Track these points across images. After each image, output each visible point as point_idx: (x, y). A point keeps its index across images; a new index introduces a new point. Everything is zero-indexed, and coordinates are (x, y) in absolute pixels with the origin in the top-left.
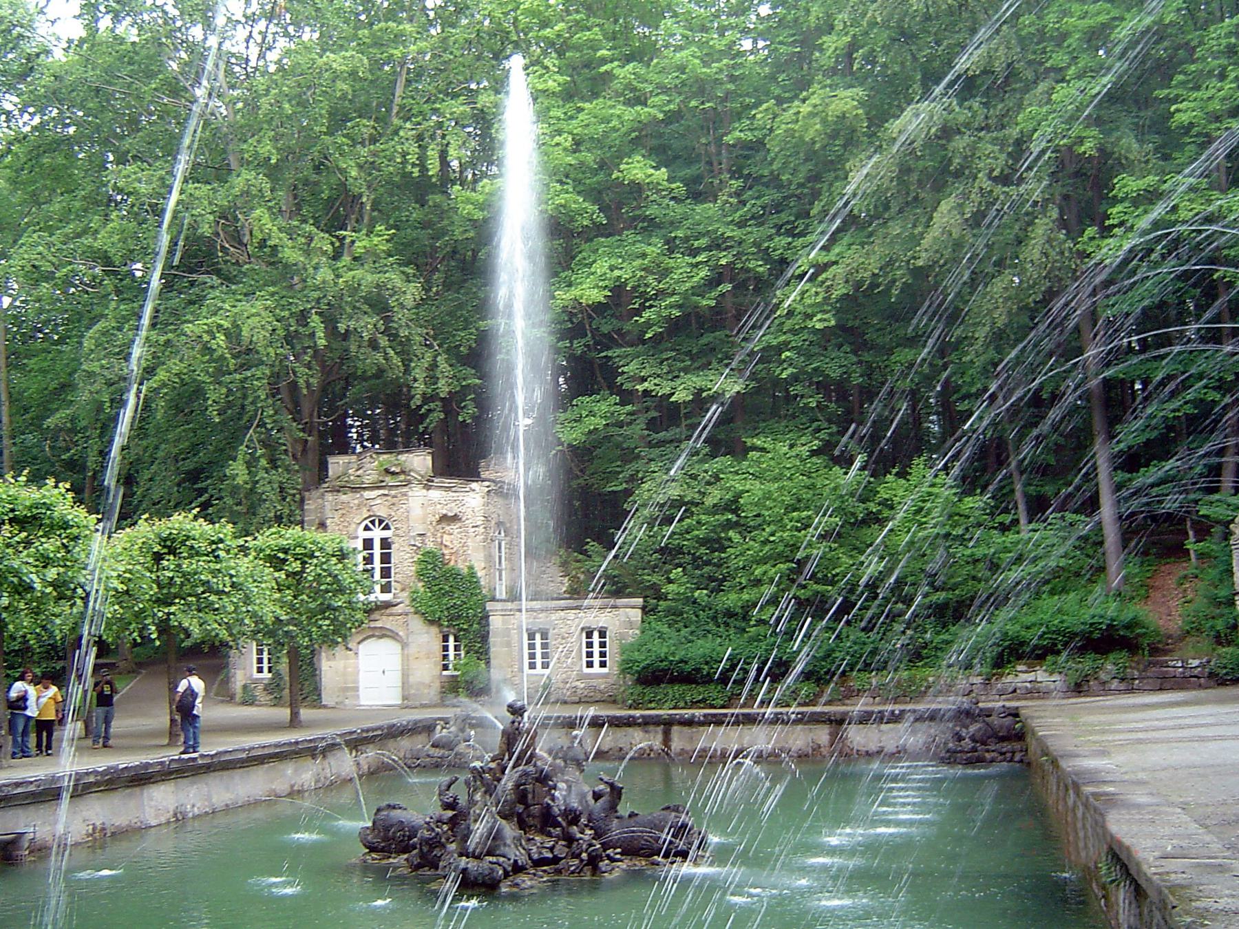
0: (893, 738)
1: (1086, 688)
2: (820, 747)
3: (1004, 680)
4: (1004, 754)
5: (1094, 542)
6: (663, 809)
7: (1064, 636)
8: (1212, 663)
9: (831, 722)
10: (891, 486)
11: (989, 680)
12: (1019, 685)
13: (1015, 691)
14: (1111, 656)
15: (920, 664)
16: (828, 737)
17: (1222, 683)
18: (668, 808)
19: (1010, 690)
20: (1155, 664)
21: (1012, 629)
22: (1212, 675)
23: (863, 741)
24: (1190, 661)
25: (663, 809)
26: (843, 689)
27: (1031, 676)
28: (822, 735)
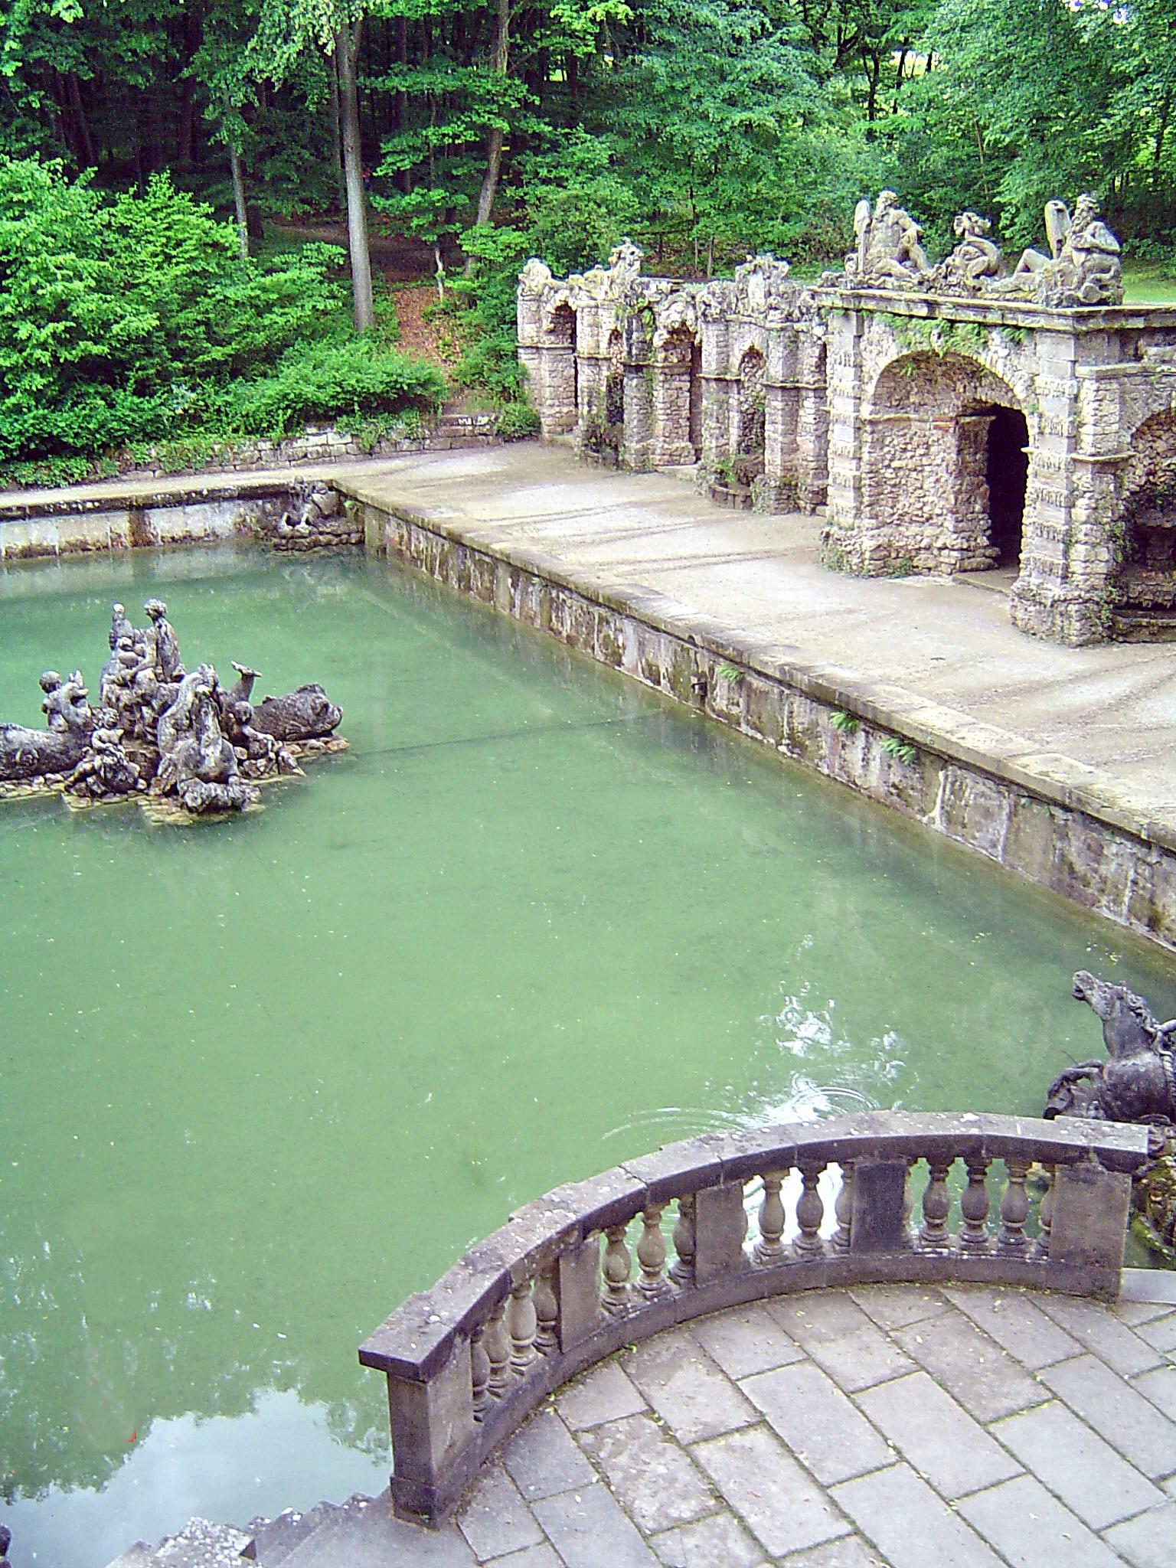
0: (199, 521)
1: (377, 449)
2: (119, 536)
3: (295, 444)
4: (340, 535)
5: (340, 272)
6: (299, 692)
7: (359, 396)
8: (500, 420)
9: (131, 507)
10: (126, 208)
11: (279, 445)
12: (310, 449)
13: (306, 456)
14: (403, 415)
15: (202, 429)
16: (128, 524)
17: (509, 440)
18: (304, 689)
19: (300, 455)
20: (445, 422)
21: (309, 391)
22: (499, 433)
23: (167, 526)
24: (480, 418)
25: (299, 692)
26: (118, 463)
27: (322, 439)
28: (122, 523)
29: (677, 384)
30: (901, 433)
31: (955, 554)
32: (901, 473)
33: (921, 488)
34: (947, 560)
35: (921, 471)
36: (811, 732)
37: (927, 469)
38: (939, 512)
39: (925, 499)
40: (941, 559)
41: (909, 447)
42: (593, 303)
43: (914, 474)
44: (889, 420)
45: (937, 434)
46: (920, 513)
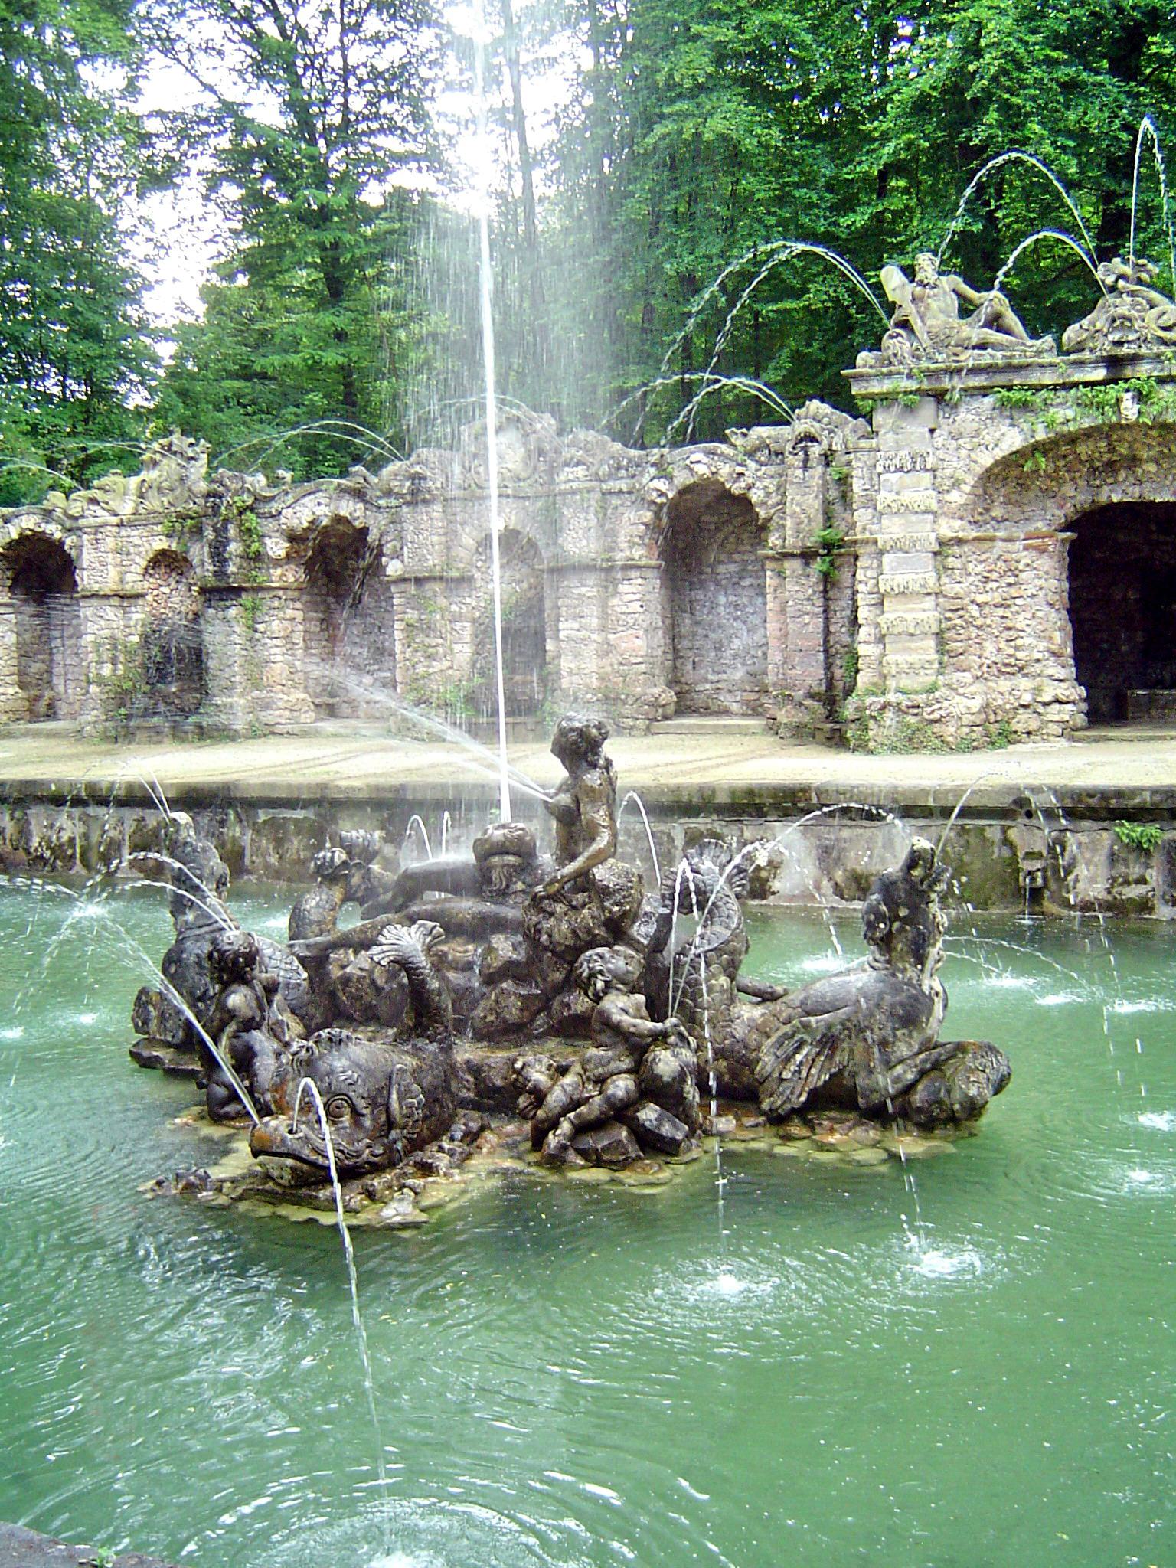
29: (290, 613)
30: (983, 557)
31: (1070, 707)
32: (987, 610)
33: (1009, 629)
34: (1056, 718)
35: (1009, 606)
37: (1018, 601)
38: (1039, 656)
39: (1019, 642)
40: (1050, 717)
41: (994, 576)
42: (115, 520)
43: (1000, 611)
44: (976, 539)
45: (1026, 557)
46: (1012, 661)
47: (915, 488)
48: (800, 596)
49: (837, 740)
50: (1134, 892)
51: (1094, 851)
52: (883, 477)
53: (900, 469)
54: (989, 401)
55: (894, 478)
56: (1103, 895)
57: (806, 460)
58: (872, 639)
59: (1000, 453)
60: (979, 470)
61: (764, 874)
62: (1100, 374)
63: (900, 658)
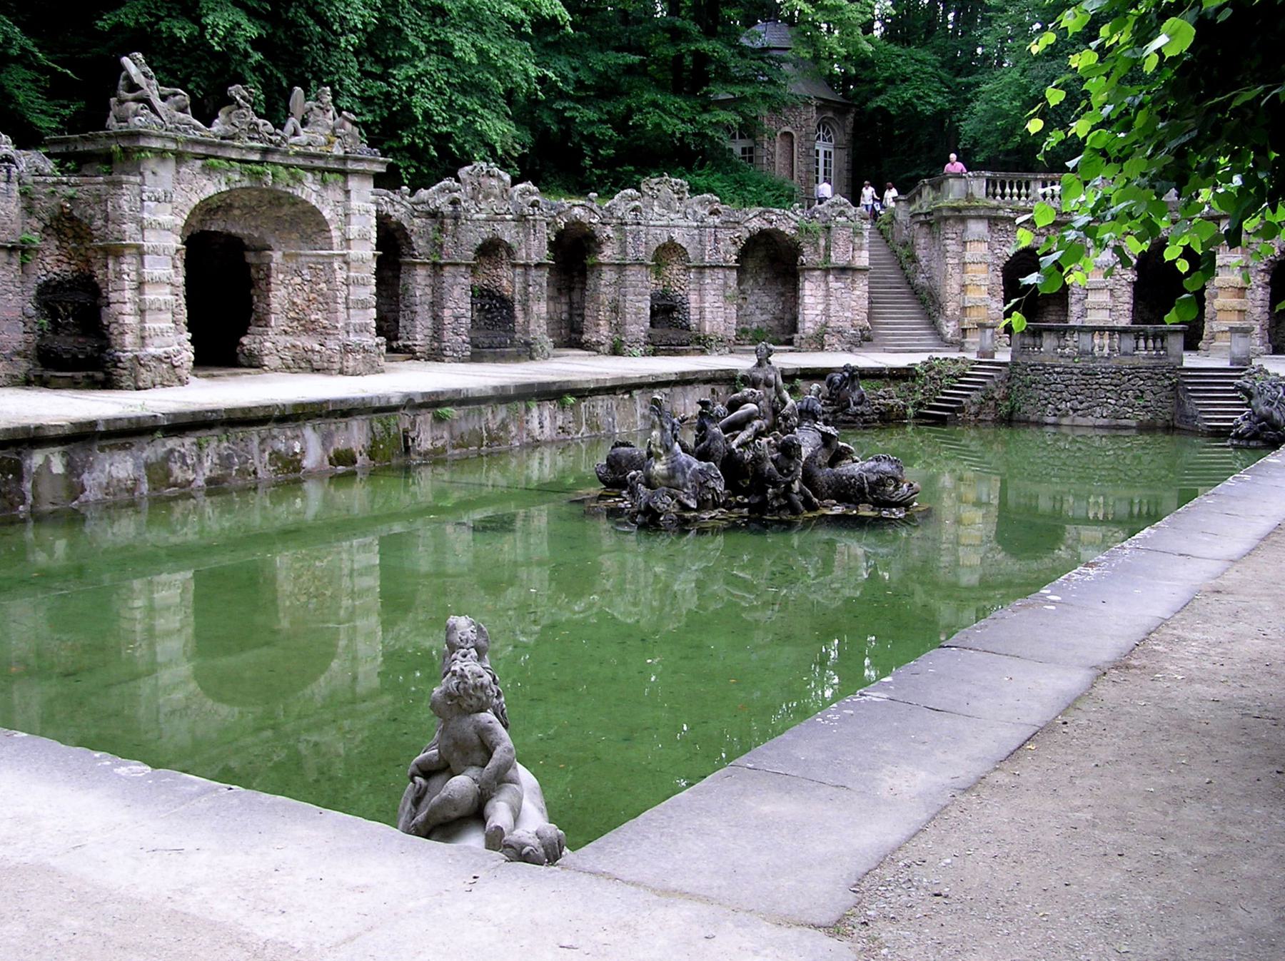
36: (504, 426)
47: (164, 212)
48: (6, 279)
49: (108, 384)
50: (439, 444)
51: (426, 423)
52: (145, 203)
53: (157, 200)
54: (199, 163)
55: (152, 204)
56: (430, 447)
57: (9, 177)
58: (133, 312)
59: (203, 197)
60: (193, 206)
61: (299, 457)
62: (256, 157)
63: (156, 326)
